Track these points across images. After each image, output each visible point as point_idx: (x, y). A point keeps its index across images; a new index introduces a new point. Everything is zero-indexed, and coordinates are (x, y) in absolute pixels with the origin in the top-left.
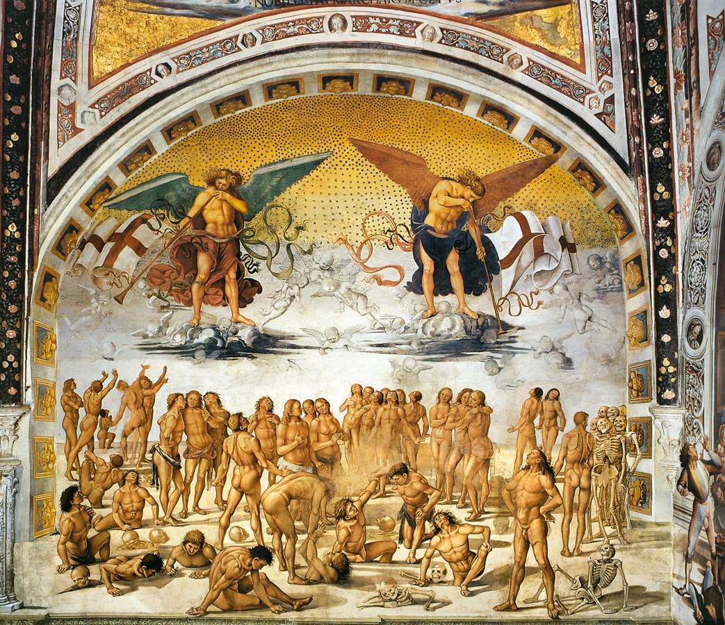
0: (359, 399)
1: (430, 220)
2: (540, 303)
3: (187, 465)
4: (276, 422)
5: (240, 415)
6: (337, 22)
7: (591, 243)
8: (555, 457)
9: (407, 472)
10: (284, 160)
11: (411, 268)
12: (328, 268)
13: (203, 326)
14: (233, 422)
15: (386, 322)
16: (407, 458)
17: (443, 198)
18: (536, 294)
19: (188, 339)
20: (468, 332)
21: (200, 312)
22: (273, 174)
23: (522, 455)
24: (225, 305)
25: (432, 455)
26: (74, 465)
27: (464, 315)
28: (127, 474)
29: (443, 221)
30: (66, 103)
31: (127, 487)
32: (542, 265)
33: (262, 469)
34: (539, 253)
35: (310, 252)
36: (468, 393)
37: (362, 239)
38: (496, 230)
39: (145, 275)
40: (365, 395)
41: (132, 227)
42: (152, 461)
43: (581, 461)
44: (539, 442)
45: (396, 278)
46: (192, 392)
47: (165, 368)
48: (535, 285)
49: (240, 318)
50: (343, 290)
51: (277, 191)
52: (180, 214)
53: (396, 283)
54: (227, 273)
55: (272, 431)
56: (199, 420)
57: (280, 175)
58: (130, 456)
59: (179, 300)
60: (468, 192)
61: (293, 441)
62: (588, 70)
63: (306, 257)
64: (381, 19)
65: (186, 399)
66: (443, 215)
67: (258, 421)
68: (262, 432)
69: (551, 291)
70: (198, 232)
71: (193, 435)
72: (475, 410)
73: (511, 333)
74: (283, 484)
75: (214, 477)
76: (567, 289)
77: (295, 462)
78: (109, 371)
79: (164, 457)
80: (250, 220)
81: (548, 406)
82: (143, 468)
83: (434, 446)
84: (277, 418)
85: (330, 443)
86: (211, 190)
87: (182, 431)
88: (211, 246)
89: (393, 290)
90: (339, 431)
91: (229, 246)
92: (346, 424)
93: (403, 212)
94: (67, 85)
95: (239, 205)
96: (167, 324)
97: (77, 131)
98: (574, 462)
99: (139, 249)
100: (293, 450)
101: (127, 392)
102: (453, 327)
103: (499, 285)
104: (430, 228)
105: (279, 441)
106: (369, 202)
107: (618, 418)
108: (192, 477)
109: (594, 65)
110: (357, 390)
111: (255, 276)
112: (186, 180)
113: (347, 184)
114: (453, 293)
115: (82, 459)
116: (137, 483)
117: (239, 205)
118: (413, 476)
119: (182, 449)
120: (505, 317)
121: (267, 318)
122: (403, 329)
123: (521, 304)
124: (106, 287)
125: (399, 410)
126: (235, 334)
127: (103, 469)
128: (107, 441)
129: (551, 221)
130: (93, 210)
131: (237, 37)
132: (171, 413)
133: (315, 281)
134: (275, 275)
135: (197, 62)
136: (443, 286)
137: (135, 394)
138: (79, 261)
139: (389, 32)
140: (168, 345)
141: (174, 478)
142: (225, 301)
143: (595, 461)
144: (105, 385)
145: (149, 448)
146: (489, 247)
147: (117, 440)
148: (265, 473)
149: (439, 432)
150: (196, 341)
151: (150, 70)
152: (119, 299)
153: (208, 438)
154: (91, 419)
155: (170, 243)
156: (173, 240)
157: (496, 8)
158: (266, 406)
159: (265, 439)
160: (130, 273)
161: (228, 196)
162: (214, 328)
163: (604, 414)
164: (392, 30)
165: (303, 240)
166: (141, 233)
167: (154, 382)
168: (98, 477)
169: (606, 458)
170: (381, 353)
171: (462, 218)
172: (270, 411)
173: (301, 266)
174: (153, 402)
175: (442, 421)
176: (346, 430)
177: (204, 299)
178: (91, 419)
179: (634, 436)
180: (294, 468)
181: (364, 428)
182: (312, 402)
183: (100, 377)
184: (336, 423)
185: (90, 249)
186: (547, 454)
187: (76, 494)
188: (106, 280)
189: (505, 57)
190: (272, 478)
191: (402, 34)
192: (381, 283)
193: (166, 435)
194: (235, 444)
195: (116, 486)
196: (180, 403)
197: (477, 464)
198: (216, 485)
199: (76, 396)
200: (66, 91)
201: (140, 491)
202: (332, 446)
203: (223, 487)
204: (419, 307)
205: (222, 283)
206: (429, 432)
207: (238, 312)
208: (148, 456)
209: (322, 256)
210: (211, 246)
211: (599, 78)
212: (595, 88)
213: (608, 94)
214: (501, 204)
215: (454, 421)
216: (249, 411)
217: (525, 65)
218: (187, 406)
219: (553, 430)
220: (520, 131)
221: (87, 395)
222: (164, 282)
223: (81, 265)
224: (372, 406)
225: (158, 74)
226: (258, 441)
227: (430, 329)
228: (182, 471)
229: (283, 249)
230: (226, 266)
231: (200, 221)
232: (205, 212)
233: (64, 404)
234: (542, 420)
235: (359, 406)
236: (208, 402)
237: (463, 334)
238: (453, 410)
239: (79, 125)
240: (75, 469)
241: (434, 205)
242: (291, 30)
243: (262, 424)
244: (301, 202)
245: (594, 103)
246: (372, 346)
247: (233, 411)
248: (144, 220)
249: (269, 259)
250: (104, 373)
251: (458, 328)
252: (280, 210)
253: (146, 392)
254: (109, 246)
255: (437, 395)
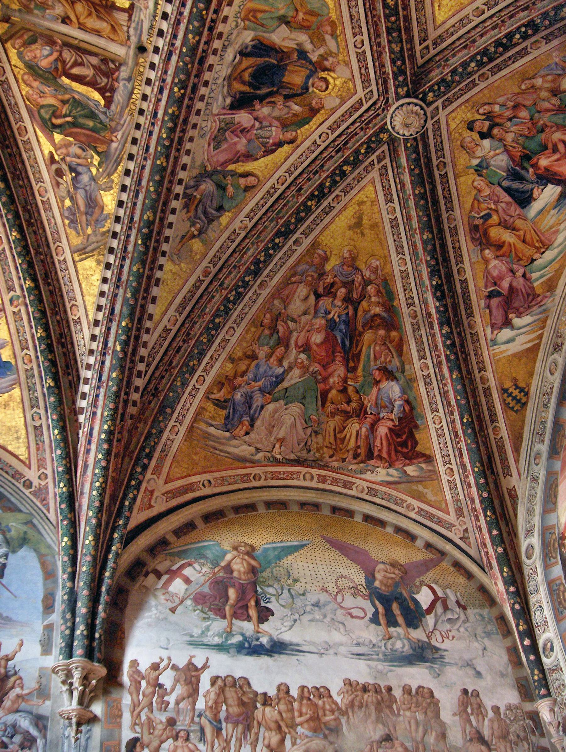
0: (350, 688)
1: (377, 584)
2: (453, 637)
3: (227, 729)
4: (292, 700)
5: (265, 694)
6: (308, 476)
7: (475, 607)
8: (486, 733)
9: (391, 740)
10: (281, 542)
11: (371, 611)
12: (317, 605)
13: (234, 633)
14: (259, 698)
15: (361, 641)
16: (389, 730)
17: (383, 573)
18: (450, 631)
19: (224, 640)
20: (414, 650)
21: (232, 623)
22: (275, 549)
23: (465, 732)
24: (249, 621)
25: (406, 729)
26: (137, 721)
27: (409, 639)
28: (179, 732)
29: (385, 585)
30: (150, 489)
31: (180, 743)
32: (449, 615)
33: (286, 734)
34: (446, 608)
35: (304, 594)
36: (421, 689)
37: (336, 591)
38: (418, 593)
39: (191, 597)
40: (354, 686)
41: (182, 567)
42: (199, 723)
43: (504, 736)
44: (474, 723)
45: (362, 614)
46: (228, 676)
47: (208, 659)
48: (448, 626)
49: (260, 630)
50: (328, 619)
51: (279, 558)
52: (215, 564)
53: (362, 618)
54: (249, 601)
55: (290, 706)
56: (234, 694)
57: (279, 550)
58: (181, 718)
59: (217, 615)
60: (397, 572)
61: (306, 714)
62: (451, 514)
63: (301, 597)
64: (333, 478)
65: (225, 680)
66: (385, 582)
67: (279, 699)
68: (282, 707)
69: (458, 630)
70: (228, 576)
71: (231, 706)
72: (428, 701)
73: (441, 653)
74: (302, 746)
75: (248, 738)
76: (467, 630)
77: (311, 729)
78: (165, 657)
79: (209, 721)
80: (262, 572)
81: (473, 700)
82: (192, 728)
83: (407, 723)
84: (293, 697)
85: (333, 717)
86: (235, 553)
87: (222, 703)
88: (237, 584)
89: (362, 622)
90: (339, 709)
91: (249, 586)
92: (343, 705)
93: (359, 578)
94: (154, 479)
95: (253, 563)
96: (207, 629)
97: (151, 506)
98: (499, 738)
99: (187, 581)
100: (307, 721)
101: (179, 673)
102: (404, 646)
103: (427, 625)
104: (376, 588)
105: (296, 714)
106: (338, 570)
107: (518, 711)
108: (232, 737)
109: (454, 512)
110: (347, 682)
111: (268, 605)
112: (219, 545)
113: (322, 559)
114: (400, 626)
115: (143, 717)
116: (187, 739)
117: (253, 563)
118: (397, 743)
119: (222, 715)
120: (434, 642)
121: (279, 631)
122: (371, 646)
123: (442, 636)
124: (163, 602)
125: (379, 697)
126: (257, 639)
127: (160, 727)
128: (163, 706)
129: (448, 591)
130: (154, 554)
131: (251, 474)
132: (213, 689)
133: (309, 612)
134: (283, 606)
135: (226, 483)
136: (392, 622)
137: (185, 674)
138: (144, 584)
139: (337, 486)
140: (209, 643)
141: (217, 737)
142: (249, 618)
143: (512, 737)
144: (162, 666)
145: (197, 713)
146: (416, 602)
147: (172, 705)
148: (288, 737)
149: (408, 713)
150: (229, 642)
151: (200, 482)
152: (173, 610)
153: (242, 709)
154: (150, 690)
155: (208, 580)
156: (211, 578)
157: (397, 479)
158: (284, 689)
159: (286, 712)
160: (181, 595)
161: (246, 557)
162: (243, 635)
163: (509, 708)
164: (339, 484)
165: (298, 588)
166: (187, 572)
167: (199, 666)
168: (157, 732)
169: (518, 736)
170: (360, 659)
171: (396, 584)
172: (288, 692)
173: (299, 602)
174: (198, 681)
175: (409, 706)
176: (344, 708)
177: (235, 615)
178: (150, 690)
179: (531, 723)
180: (307, 733)
181: (356, 708)
182: (317, 688)
183: (158, 660)
184: (336, 703)
185: (152, 577)
186: (481, 731)
187: (138, 744)
188: (163, 597)
189: (405, 505)
190: (293, 740)
191: (345, 487)
192: (352, 617)
193: (210, 704)
194: (263, 715)
195: (170, 741)
196: (220, 682)
197: (437, 736)
198: (251, 744)
199: (138, 672)
200: (152, 482)
201: (190, 745)
202: (335, 720)
203: (256, 746)
204: (379, 633)
205: (246, 607)
206: (401, 712)
207: (258, 627)
208: (196, 719)
209: (312, 598)
210: (237, 584)
211: (458, 519)
212: (456, 523)
213: (464, 527)
214: (418, 579)
215: (416, 707)
216: (272, 692)
217: (416, 510)
218: (225, 685)
219: (480, 717)
220: (419, 543)
221: (147, 672)
222: (205, 602)
223: (145, 586)
224: (359, 693)
225: (203, 485)
226: (280, 713)
227: (389, 646)
228: (224, 732)
229: (285, 591)
230: (248, 598)
231: (228, 569)
232: (232, 564)
233: (131, 677)
234: (472, 709)
235: (350, 693)
236: (241, 683)
237: (411, 651)
238: (414, 699)
239: (152, 503)
240: (138, 725)
241: (378, 576)
242: (282, 476)
243: (282, 702)
244: (295, 566)
245: (457, 532)
246: (353, 654)
247: (260, 691)
248: (190, 565)
249: (278, 596)
250: (161, 658)
251: (407, 647)
252: (281, 569)
253: (193, 673)
254: (165, 577)
255: (401, 689)
